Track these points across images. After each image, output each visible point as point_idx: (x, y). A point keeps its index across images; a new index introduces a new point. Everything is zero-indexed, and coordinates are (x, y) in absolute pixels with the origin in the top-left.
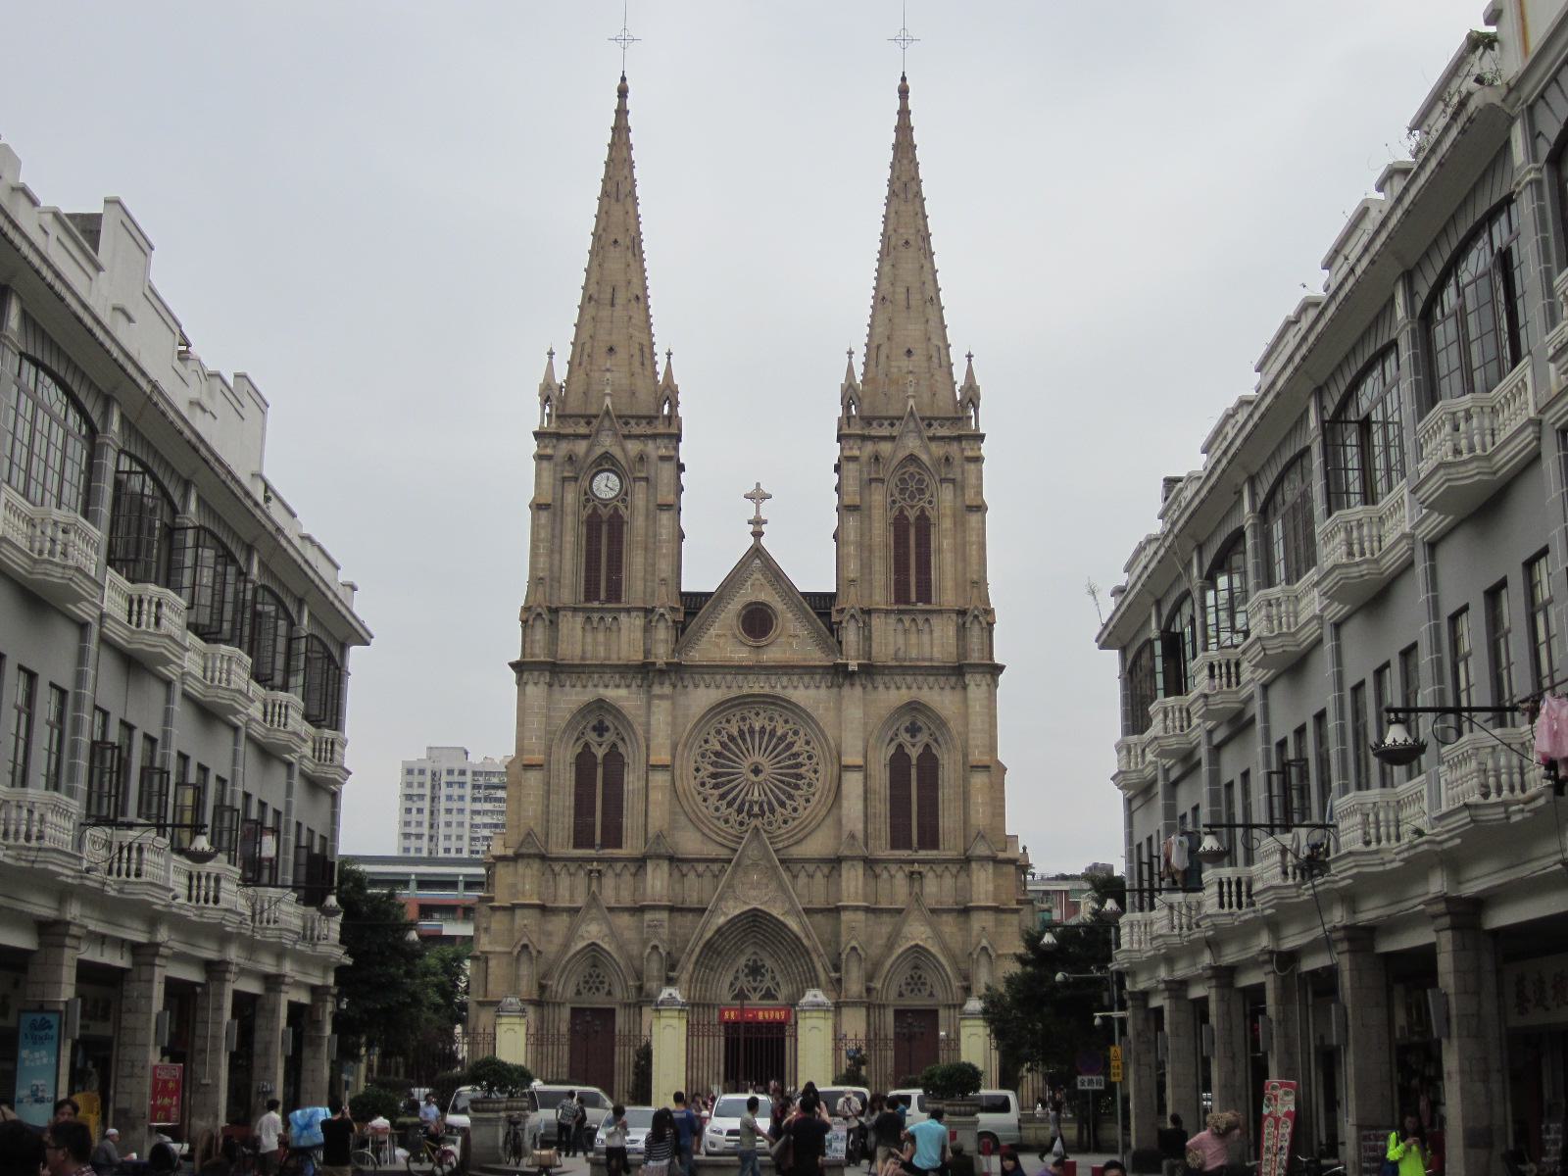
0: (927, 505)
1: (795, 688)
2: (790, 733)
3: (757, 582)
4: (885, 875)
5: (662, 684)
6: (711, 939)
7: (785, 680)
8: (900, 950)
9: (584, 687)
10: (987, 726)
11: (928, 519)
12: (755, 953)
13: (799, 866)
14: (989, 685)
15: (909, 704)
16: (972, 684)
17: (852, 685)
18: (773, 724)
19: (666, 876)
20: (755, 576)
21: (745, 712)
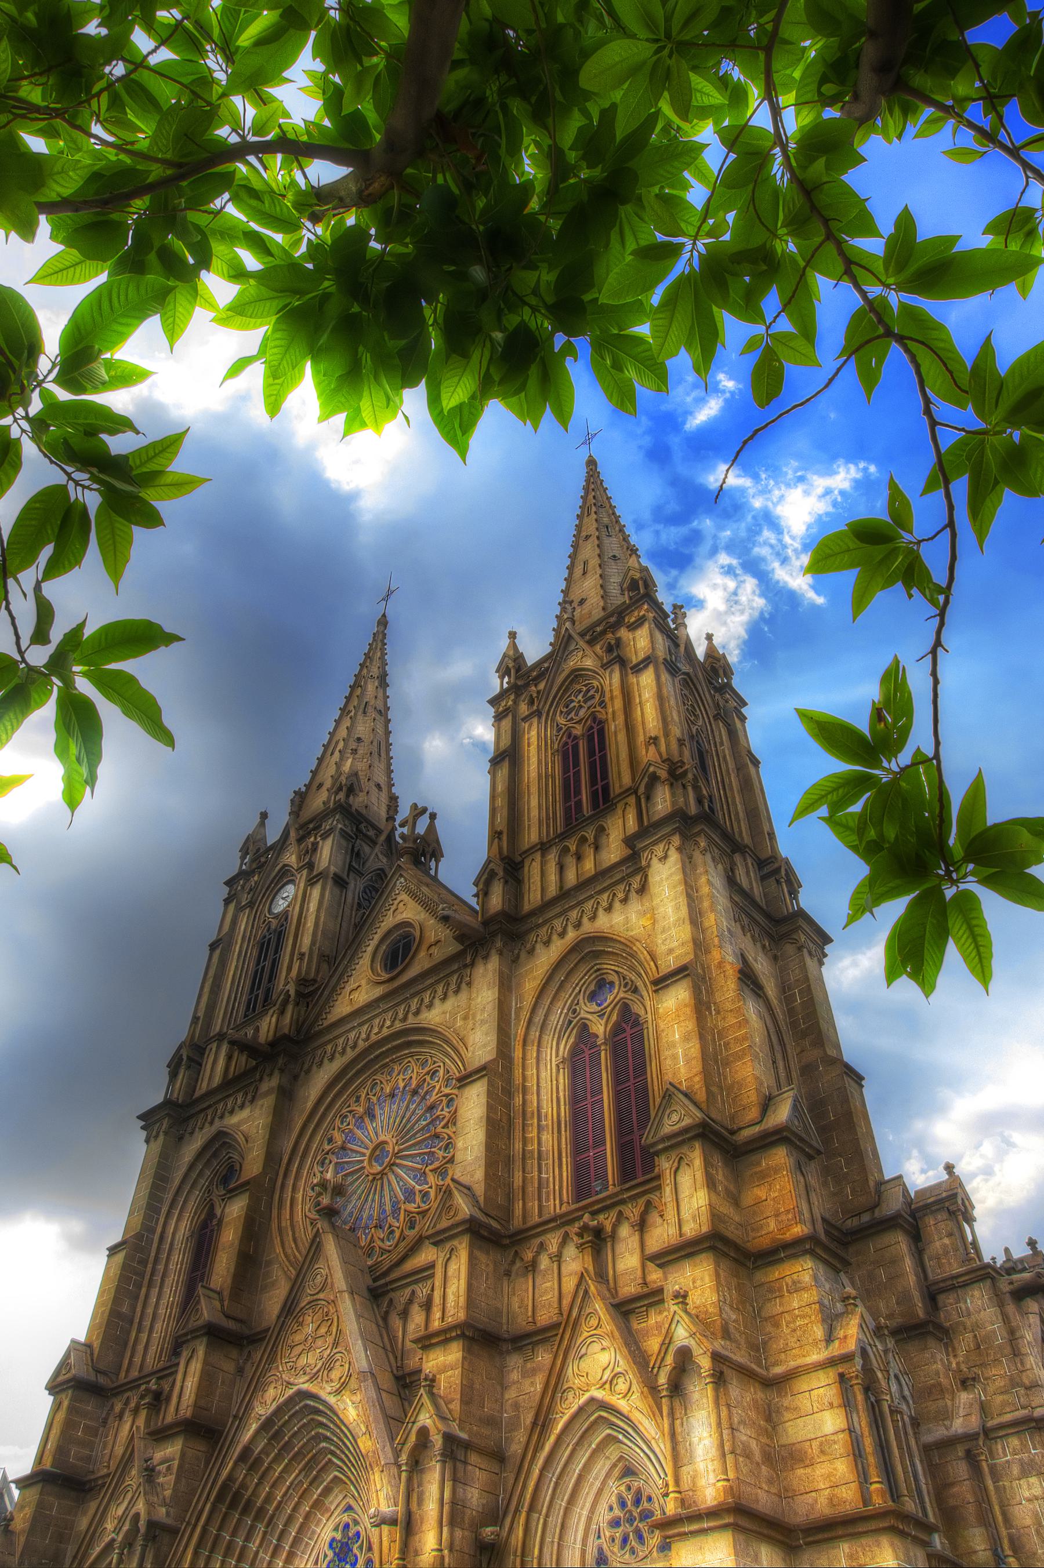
0: (598, 708)
1: (430, 1006)
2: (428, 1078)
3: (401, 904)
4: (544, 1262)
5: (271, 1075)
6: (230, 1478)
7: (414, 1004)
8: (560, 1425)
9: (211, 1123)
10: (684, 911)
11: (600, 722)
12: (349, 1508)
13: (408, 1291)
14: (679, 849)
15: (575, 948)
16: (655, 862)
17: (486, 958)
18: (408, 1077)
19: (199, 1366)
20: (399, 898)
21: (378, 1077)
